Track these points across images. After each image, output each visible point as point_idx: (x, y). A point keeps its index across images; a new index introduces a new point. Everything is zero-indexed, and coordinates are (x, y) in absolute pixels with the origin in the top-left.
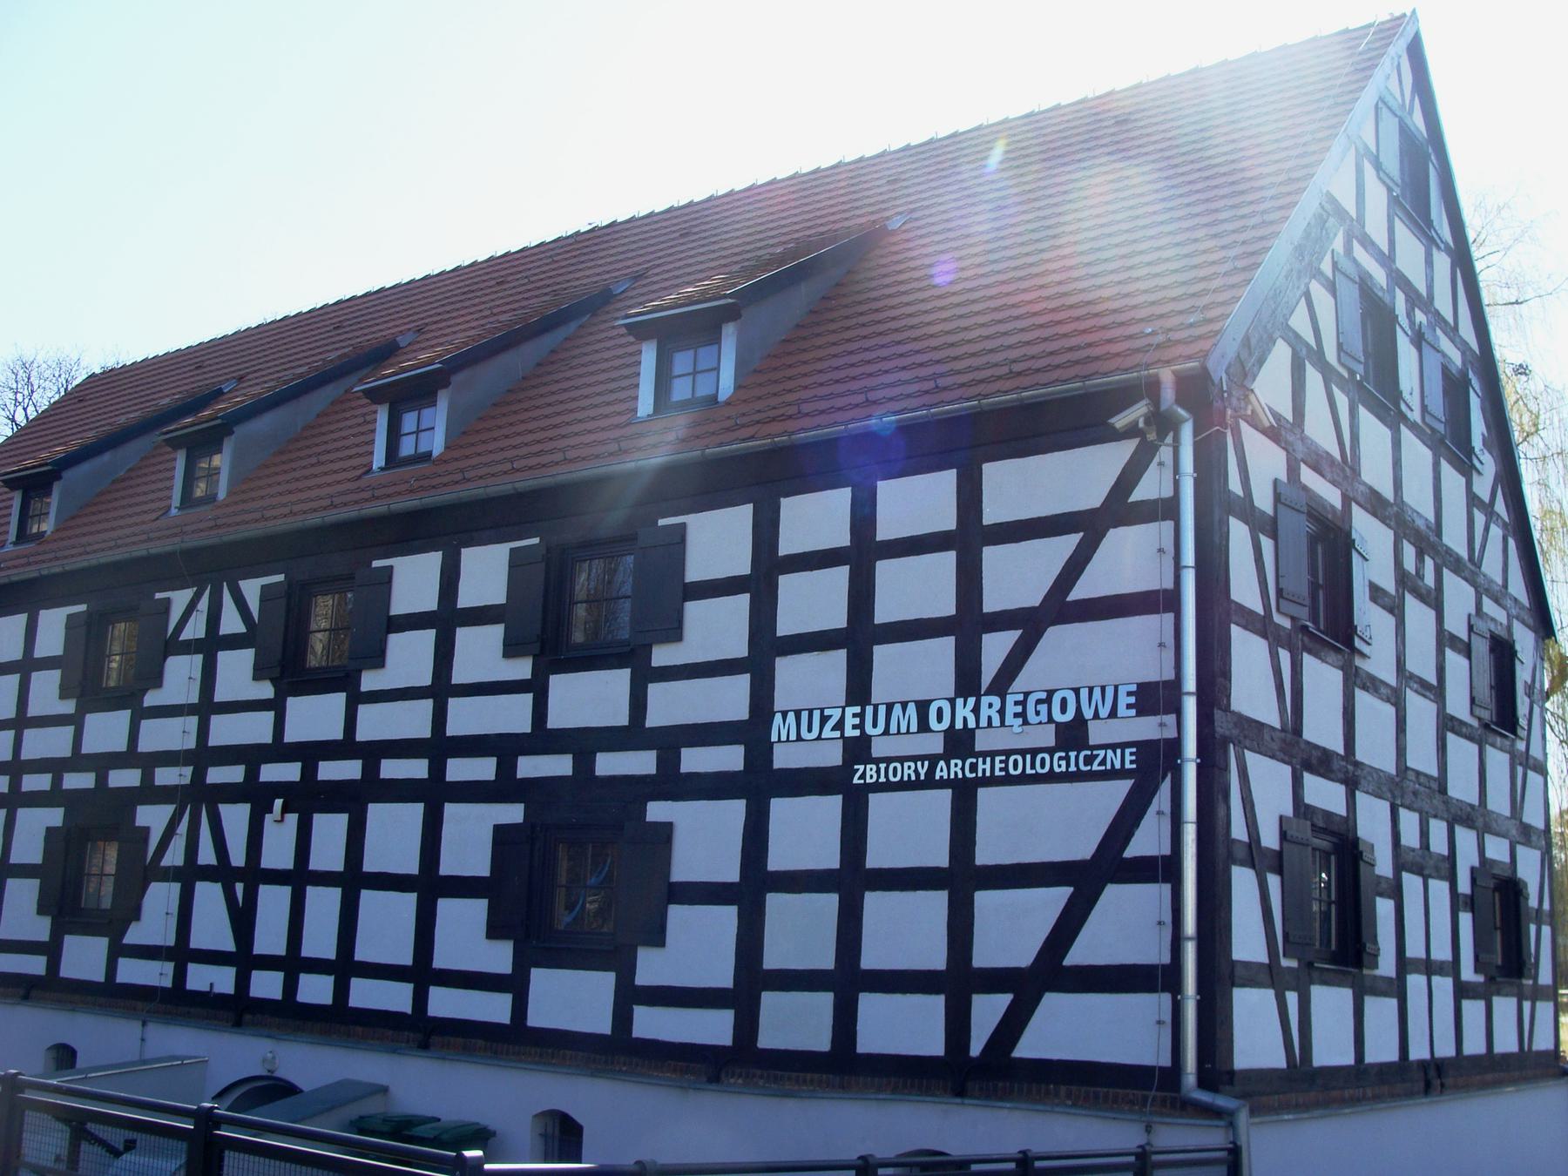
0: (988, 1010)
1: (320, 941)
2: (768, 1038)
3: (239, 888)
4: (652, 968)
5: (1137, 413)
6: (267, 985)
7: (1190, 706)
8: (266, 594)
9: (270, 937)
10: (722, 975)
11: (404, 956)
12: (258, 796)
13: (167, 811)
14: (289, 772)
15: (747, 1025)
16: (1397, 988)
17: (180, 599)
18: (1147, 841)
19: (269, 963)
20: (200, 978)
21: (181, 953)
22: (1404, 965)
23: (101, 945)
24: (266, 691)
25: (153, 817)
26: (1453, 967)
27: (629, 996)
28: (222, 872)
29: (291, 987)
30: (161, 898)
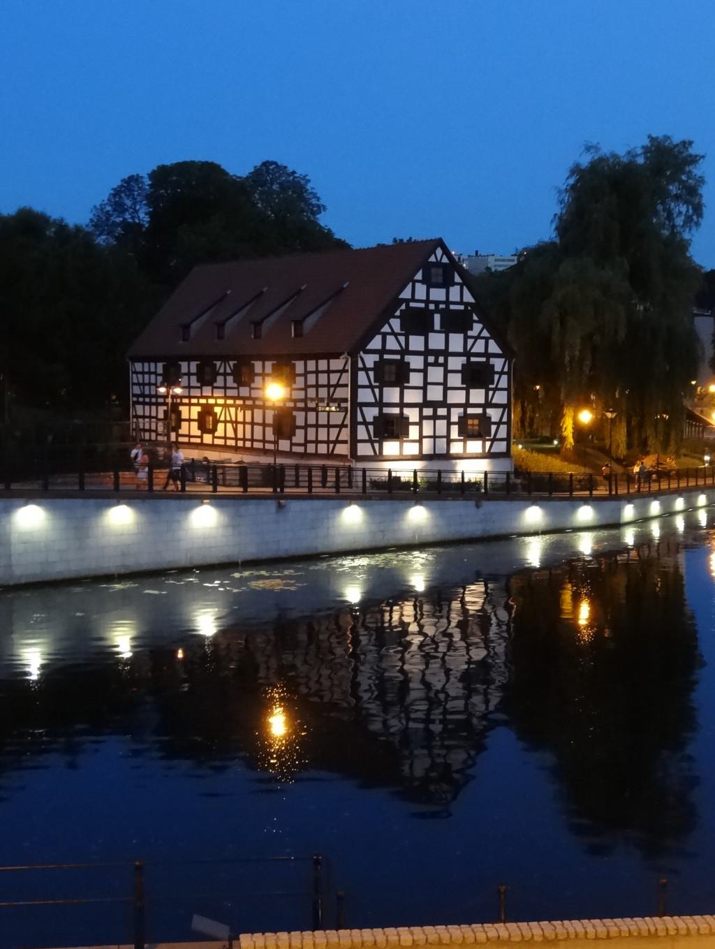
0: (331, 446)
1: (248, 436)
2: (308, 451)
3: (234, 425)
4: (295, 440)
5: (343, 356)
6: (240, 444)
7: (349, 402)
8: (234, 365)
9: (240, 435)
10: (303, 442)
11: (261, 438)
12: (236, 407)
13: (220, 408)
14: (239, 402)
15: (306, 449)
16: (420, 441)
17: (218, 363)
18: (345, 423)
19: (240, 439)
20: (230, 443)
21: (225, 438)
22: (421, 437)
23: (210, 436)
24: (235, 385)
25: (217, 410)
26: (448, 436)
27: (292, 444)
28: (231, 422)
29: (244, 444)
30: (220, 427)
